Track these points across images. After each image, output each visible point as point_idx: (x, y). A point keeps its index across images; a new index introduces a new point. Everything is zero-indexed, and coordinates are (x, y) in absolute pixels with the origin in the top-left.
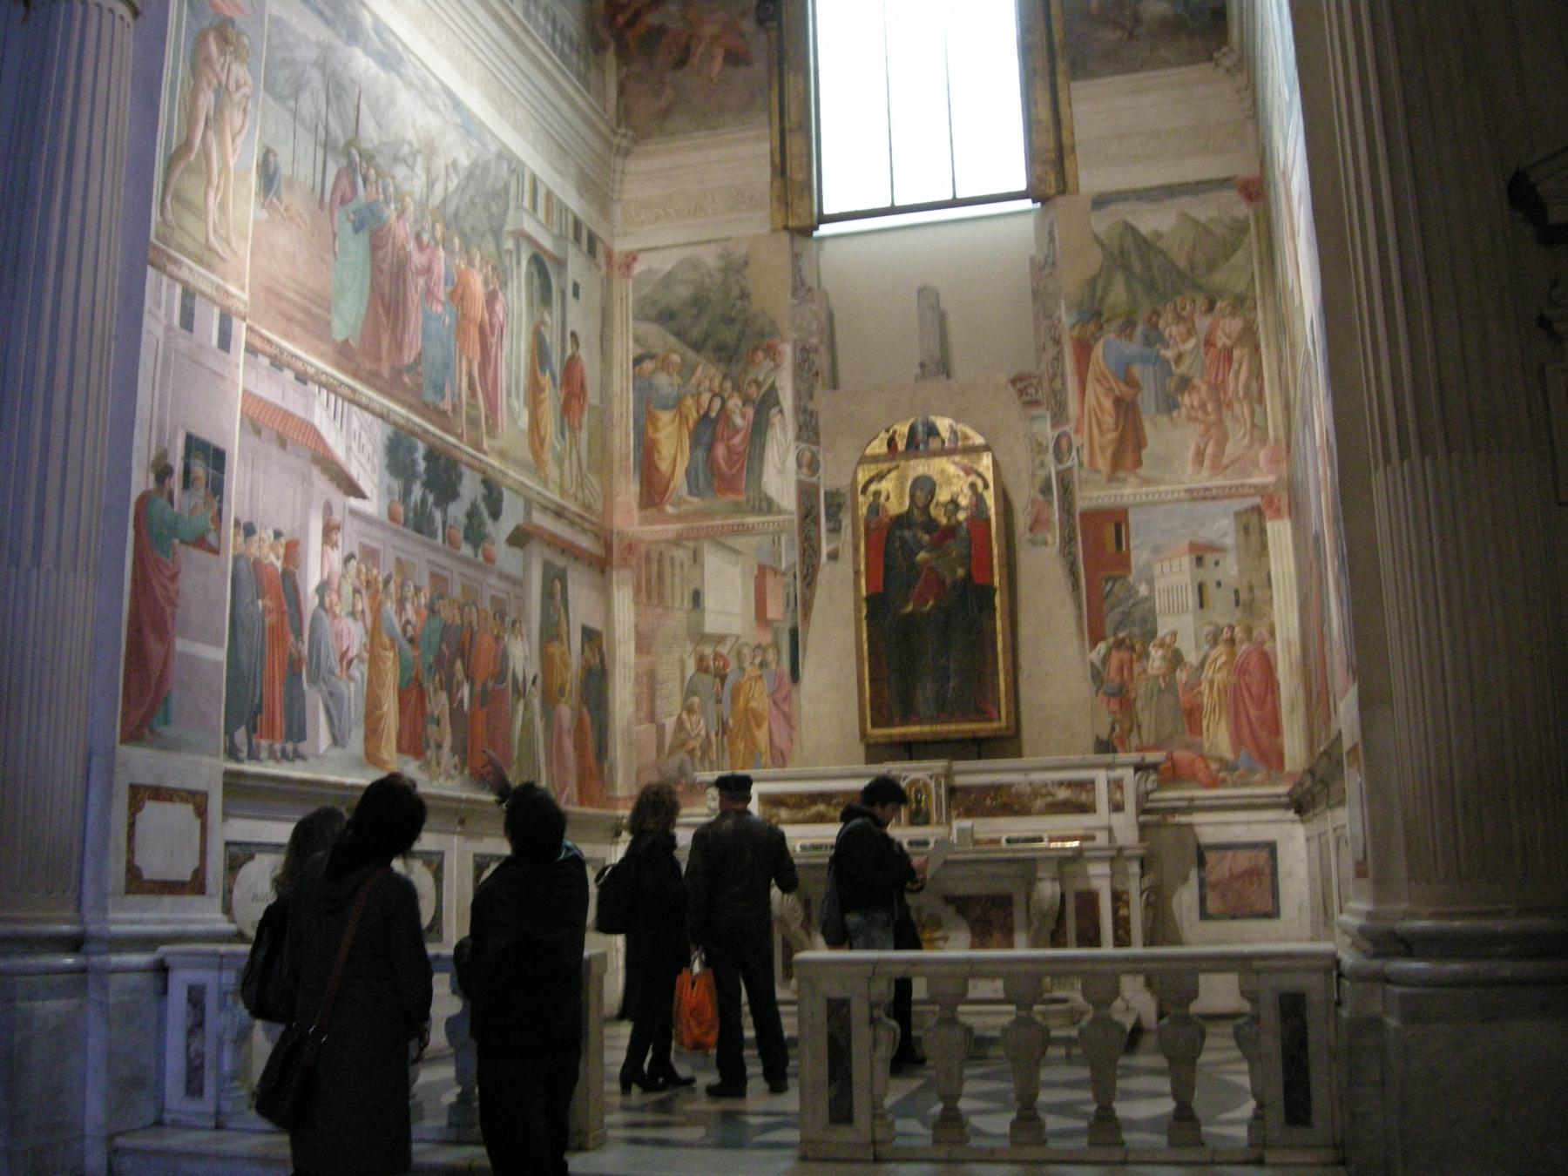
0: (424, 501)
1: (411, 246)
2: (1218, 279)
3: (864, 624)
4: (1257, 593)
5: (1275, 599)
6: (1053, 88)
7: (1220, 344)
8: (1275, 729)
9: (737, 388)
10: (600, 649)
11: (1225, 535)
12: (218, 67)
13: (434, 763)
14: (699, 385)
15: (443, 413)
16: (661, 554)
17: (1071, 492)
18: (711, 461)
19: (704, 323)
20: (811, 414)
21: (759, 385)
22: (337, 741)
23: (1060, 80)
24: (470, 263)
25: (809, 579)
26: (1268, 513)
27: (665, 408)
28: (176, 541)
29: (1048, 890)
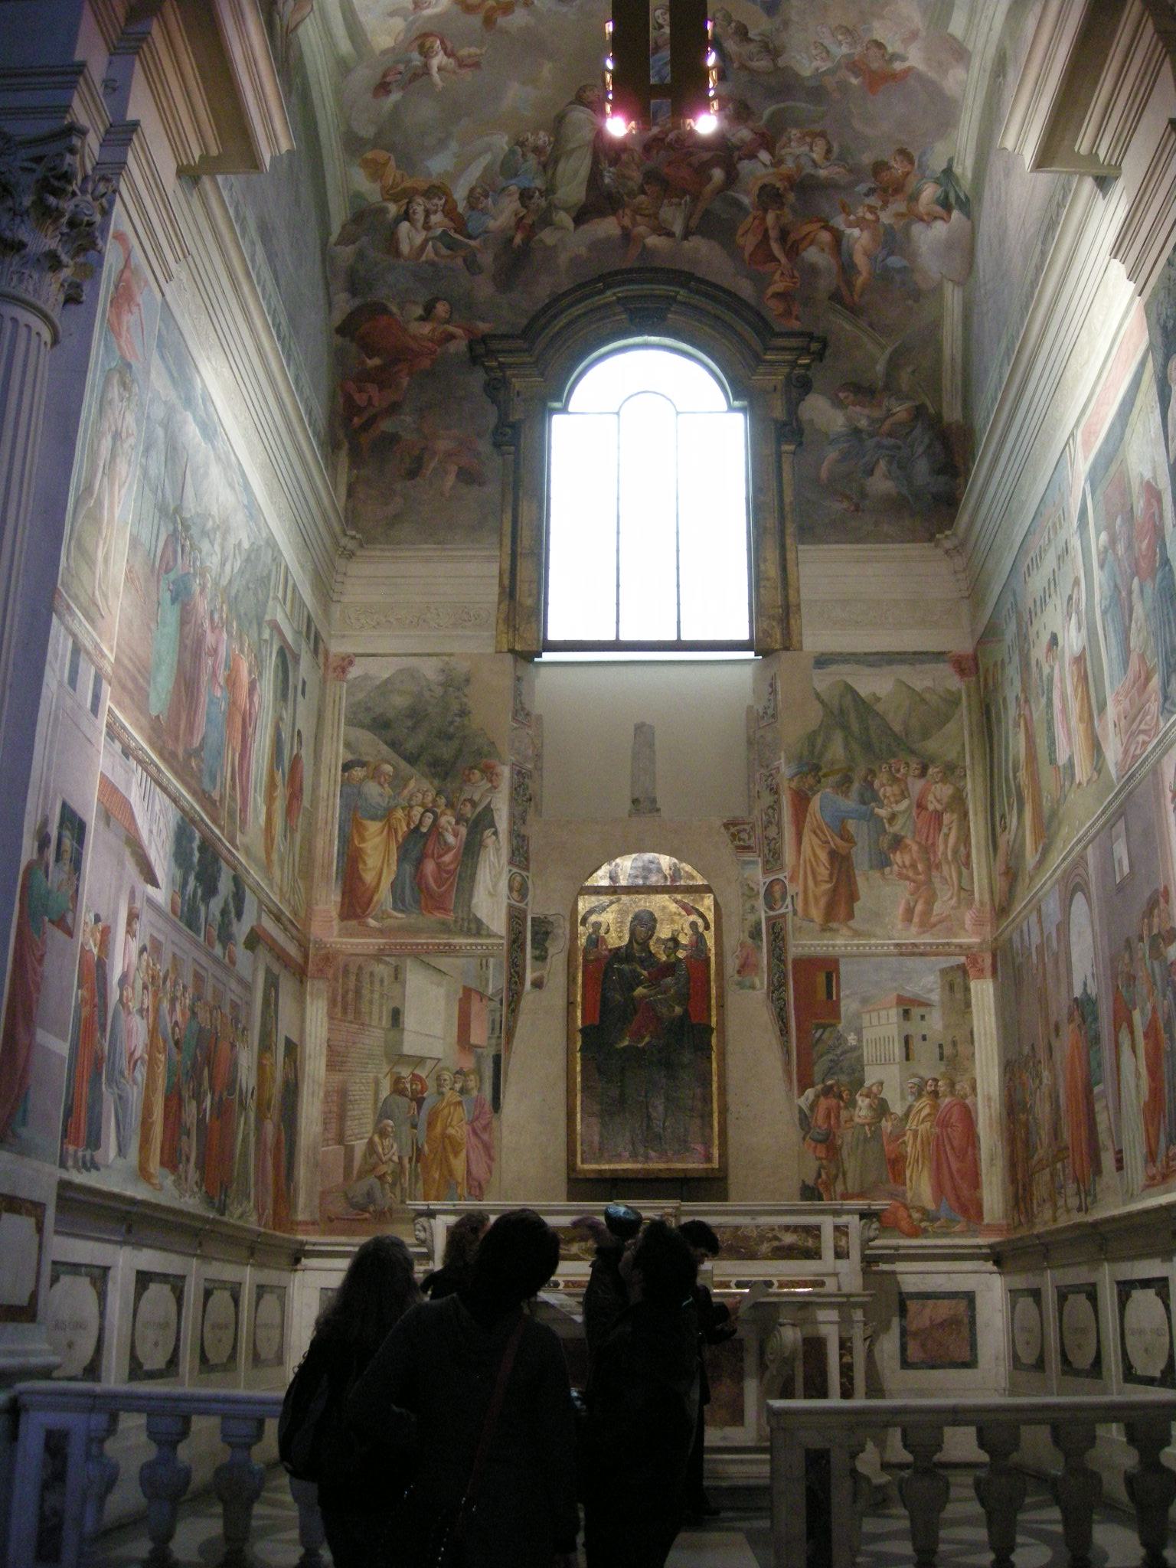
1: (207, 625)
2: (932, 746)
4: (960, 1048)
5: (977, 1056)
6: (783, 547)
7: (931, 807)
8: (976, 1184)
9: (450, 805)
10: (295, 1063)
11: (931, 990)
12: (117, 413)
14: (410, 799)
15: (214, 803)
16: (360, 968)
17: (783, 939)
19: (421, 737)
21: (474, 804)
22: (121, 1151)
23: (789, 541)
24: (241, 650)
25: (513, 1006)
26: (971, 972)
27: (373, 818)
28: (46, 919)
29: (790, 1336)
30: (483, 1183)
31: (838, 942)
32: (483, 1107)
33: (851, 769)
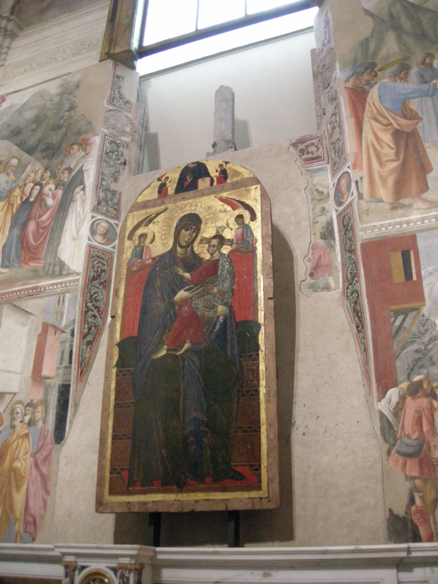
3: (114, 370)
9: (53, 176)
14: (26, 179)
17: (352, 229)
18: (23, 238)
19: (39, 134)
20: (114, 193)
21: (70, 170)
25: (89, 338)
30: (38, 519)
31: (412, 217)
32: (45, 438)
33: (406, 58)
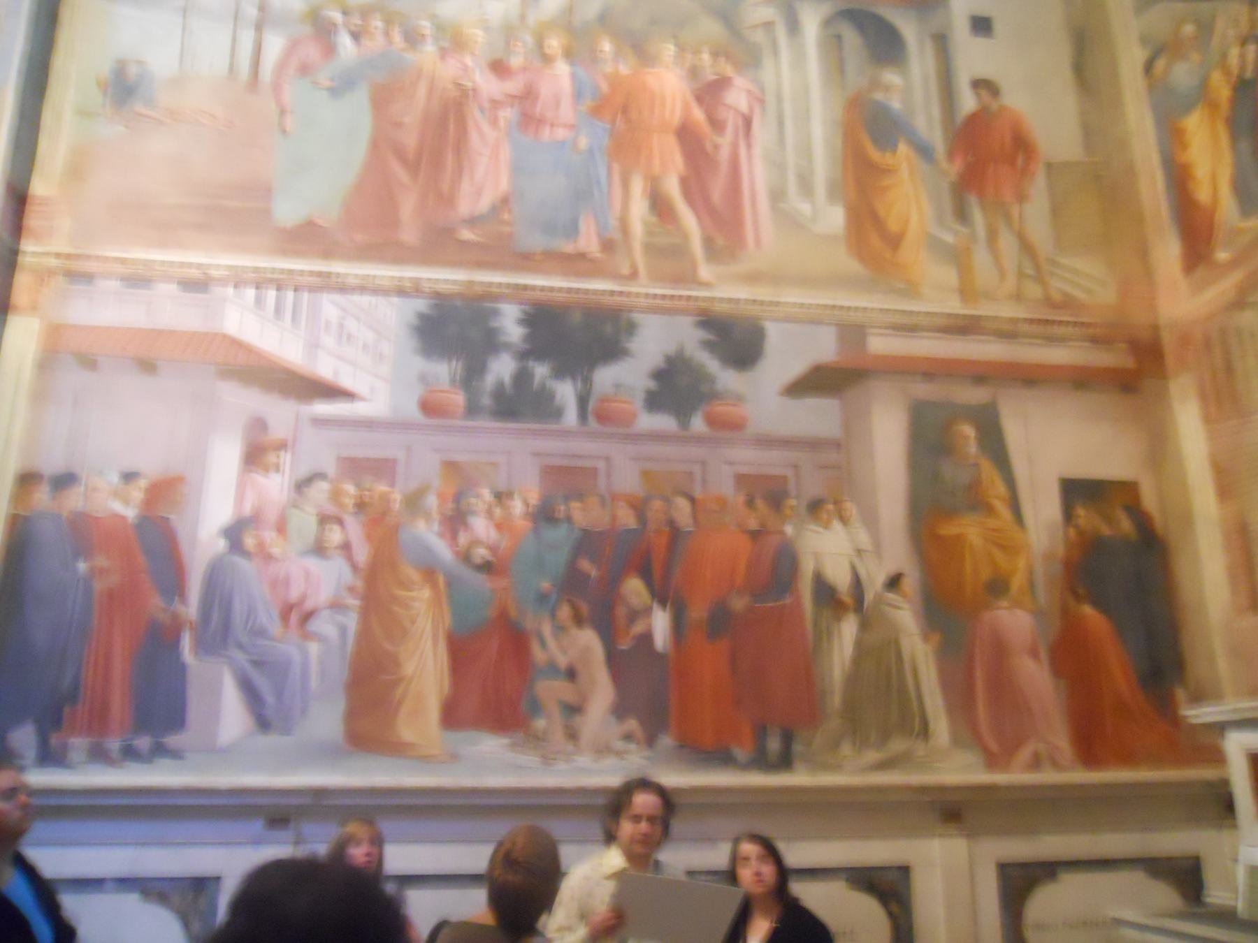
0: (522, 378)
13: (558, 735)
15: (582, 256)
27: (1188, 108)
